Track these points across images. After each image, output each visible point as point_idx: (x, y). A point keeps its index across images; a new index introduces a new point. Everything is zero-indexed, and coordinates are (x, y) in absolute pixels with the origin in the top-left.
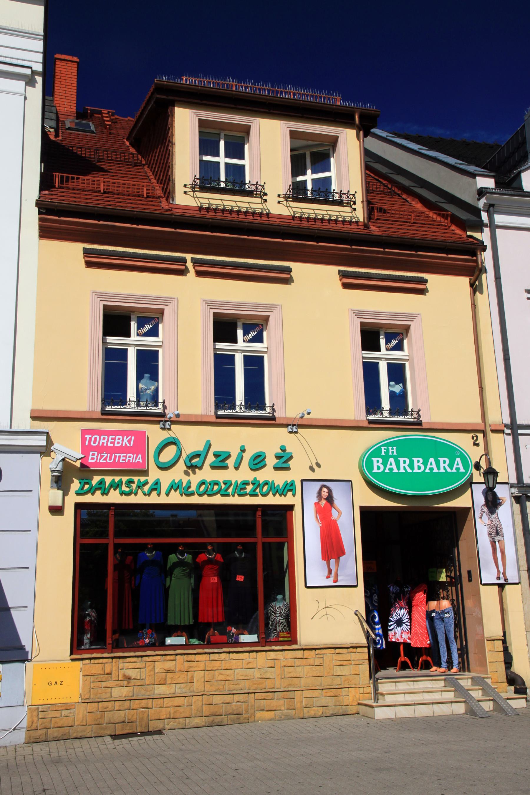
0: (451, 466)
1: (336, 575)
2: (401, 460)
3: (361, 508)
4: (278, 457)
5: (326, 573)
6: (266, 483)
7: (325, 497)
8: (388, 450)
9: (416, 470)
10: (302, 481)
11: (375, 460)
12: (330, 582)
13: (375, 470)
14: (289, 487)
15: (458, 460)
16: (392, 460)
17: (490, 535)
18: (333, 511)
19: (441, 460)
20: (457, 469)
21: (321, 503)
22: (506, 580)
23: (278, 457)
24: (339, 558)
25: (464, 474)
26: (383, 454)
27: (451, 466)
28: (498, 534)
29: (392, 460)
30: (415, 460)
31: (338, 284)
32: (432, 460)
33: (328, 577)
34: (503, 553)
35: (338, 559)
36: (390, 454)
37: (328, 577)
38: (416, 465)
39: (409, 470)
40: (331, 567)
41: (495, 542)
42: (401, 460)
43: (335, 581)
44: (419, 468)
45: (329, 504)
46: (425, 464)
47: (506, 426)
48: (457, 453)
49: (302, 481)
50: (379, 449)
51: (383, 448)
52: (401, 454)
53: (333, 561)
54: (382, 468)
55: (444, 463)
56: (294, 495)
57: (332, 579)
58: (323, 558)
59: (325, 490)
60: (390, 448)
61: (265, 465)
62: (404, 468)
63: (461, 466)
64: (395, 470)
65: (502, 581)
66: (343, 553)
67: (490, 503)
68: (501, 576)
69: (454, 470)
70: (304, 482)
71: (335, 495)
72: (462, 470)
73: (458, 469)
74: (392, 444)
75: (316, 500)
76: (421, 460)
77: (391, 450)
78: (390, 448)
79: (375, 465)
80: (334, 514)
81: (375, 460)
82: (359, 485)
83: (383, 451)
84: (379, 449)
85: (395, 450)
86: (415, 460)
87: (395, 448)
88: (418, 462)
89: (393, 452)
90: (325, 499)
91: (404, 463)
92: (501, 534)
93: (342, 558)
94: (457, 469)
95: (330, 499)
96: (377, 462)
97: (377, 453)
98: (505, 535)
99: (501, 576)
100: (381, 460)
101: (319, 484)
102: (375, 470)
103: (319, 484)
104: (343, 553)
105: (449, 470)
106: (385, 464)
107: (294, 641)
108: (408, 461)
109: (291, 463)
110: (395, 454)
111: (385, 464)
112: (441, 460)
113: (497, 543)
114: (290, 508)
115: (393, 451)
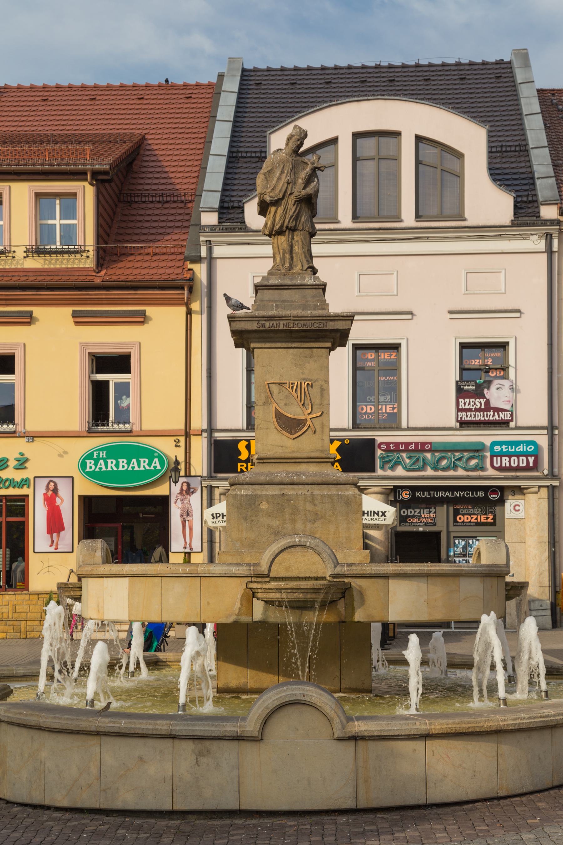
0: (149, 464)
1: (57, 544)
2: (109, 461)
3: (80, 497)
4: (18, 460)
5: (50, 543)
6: (7, 480)
7: (51, 489)
8: (99, 454)
9: (121, 468)
10: (35, 478)
11: (88, 462)
12: (52, 549)
13: (88, 469)
14: (25, 482)
15: (156, 460)
16: (102, 461)
17: (182, 516)
18: (58, 499)
19: (142, 460)
20: (154, 467)
21: (48, 494)
22: (191, 549)
23: (18, 460)
24: (59, 533)
25: (159, 471)
26: (95, 457)
27: (149, 465)
28: (188, 515)
29: (102, 461)
30: (121, 461)
31: (71, 320)
32: (134, 460)
33: (51, 546)
34: (191, 529)
35: (58, 532)
36: (101, 456)
37: (51, 546)
38: (121, 464)
39: (115, 469)
40: (54, 539)
41: (185, 521)
42: (109, 461)
43: (56, 549)
44: (123, 467)
45: (54, 494)
46: (128, 464)
47: (202, 431)
48: (156, 454)
49: (35, 478)
50: (92, 454)
51: (95, 453)
52: (109, 456)
53: (55, 535)
54: (93, 467)
55: (144, 463)
56: (29, 487)
57: (54, 547)
58: (48, 533)
59: (52, 484)
60: (101, 452)
61: (8, 466)
62: (112, 467)
63: (158, 465)
64: (104, 469)
65: (188, 550)
66: (63, 529)
67: (184, 492)
68: (188, 546)
69: (152, 468)
70: (36, 479)
71: (60, 487)
72: (159, 467)
73: (155, 467)
74: (102, 450)
75: (44, 491)
76: (125, 461)
77: (101, 454)
78: (101, 452)
79: (88, 465)
80: (58, 501)
81: (88, 462)
82: (79, 480)
83: (95, 455)
84: (92, 454)
85: (104, 454)
86: (121, 461)
87: (105, 452)
88: (123, 462)
89: (103, 456)
90: (52, 491)
91: (111, 464)
92: (190, 515)
93: (62, 533)
94: (154, 467)
95: (55, 491)
96: (90, 464)
97: (90, 456)
98: (194, 516)
99: (188, 546)
100: (93, 462)
101: (47, 480)
102: (88, 469)
103: (47, 480)
104: (63, 529)
105: (147, 468)
106: (96, 464)
107: (27, 588)
108: (114, 462)
109: (26, 465)
110: (105, 456)
111: (96, 464)
112: (142, 460)
113: (187, 522)
114: (25, 498)
115: (103, 454)
